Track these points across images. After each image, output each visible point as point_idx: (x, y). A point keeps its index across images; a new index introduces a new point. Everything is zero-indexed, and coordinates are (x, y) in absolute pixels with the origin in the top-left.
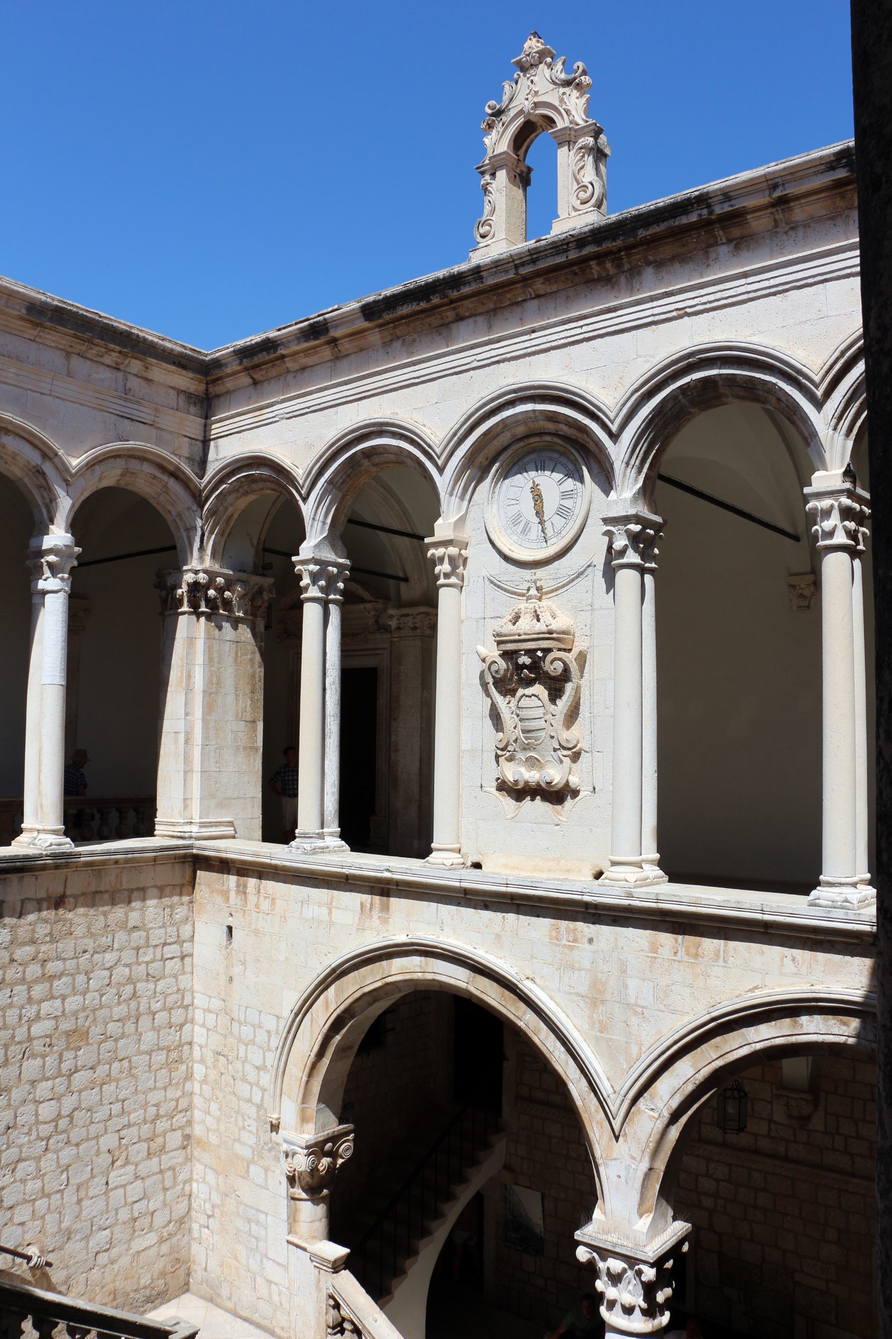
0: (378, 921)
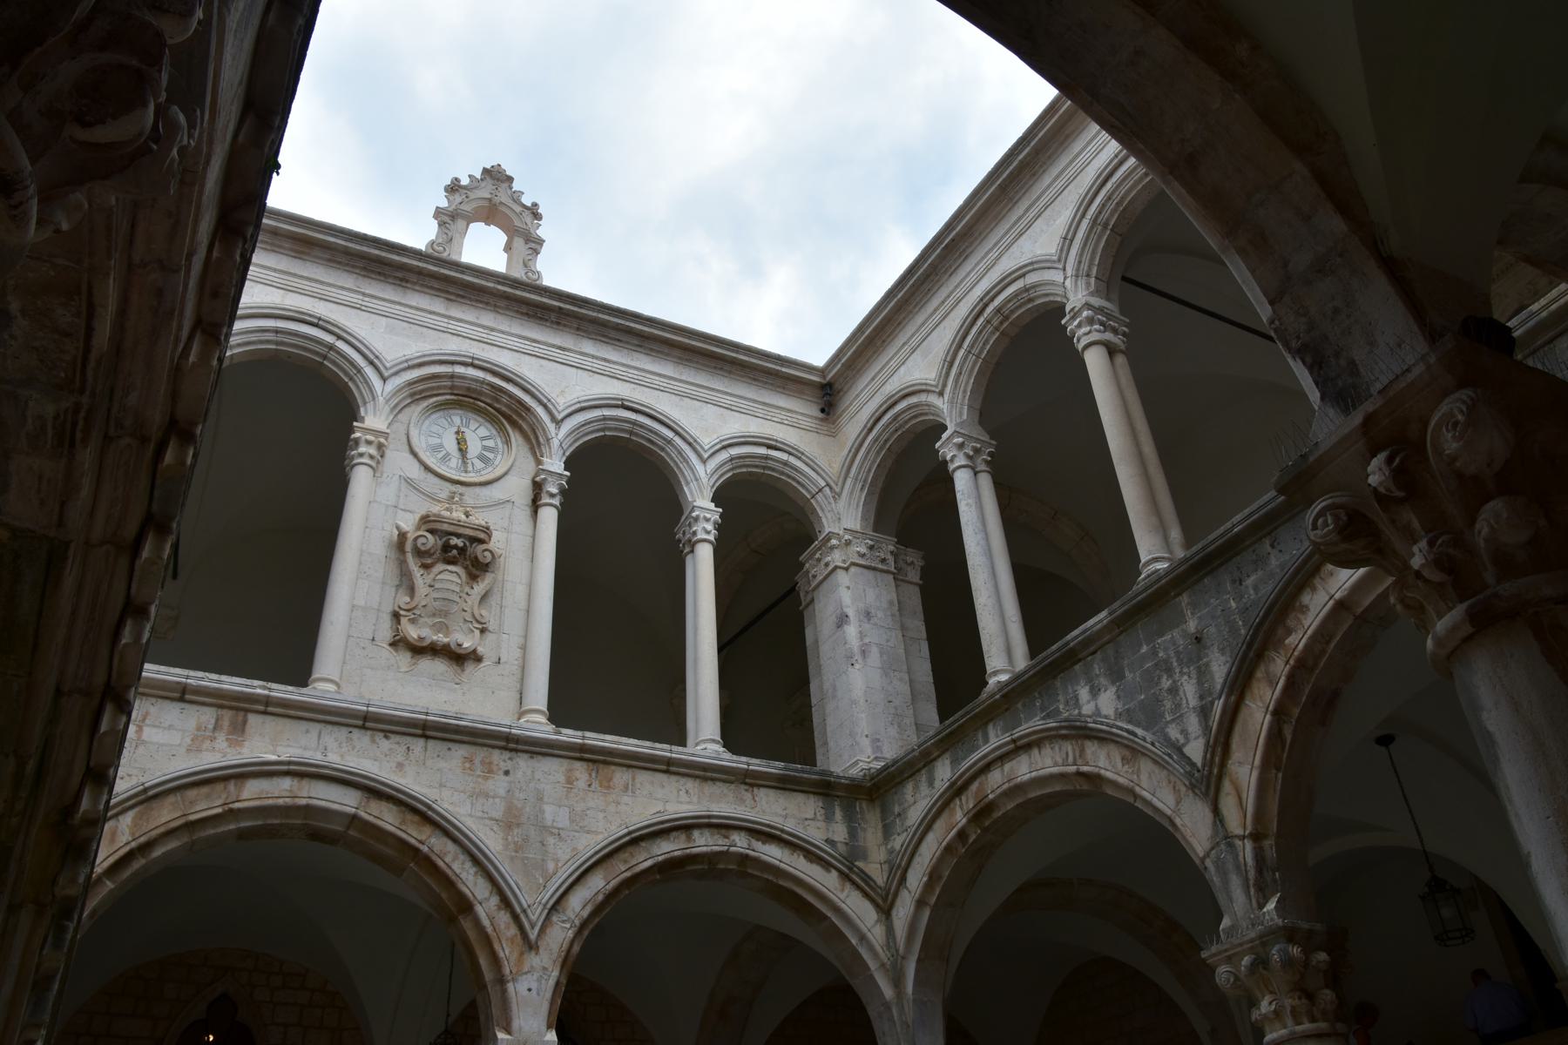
0: (225, 744)
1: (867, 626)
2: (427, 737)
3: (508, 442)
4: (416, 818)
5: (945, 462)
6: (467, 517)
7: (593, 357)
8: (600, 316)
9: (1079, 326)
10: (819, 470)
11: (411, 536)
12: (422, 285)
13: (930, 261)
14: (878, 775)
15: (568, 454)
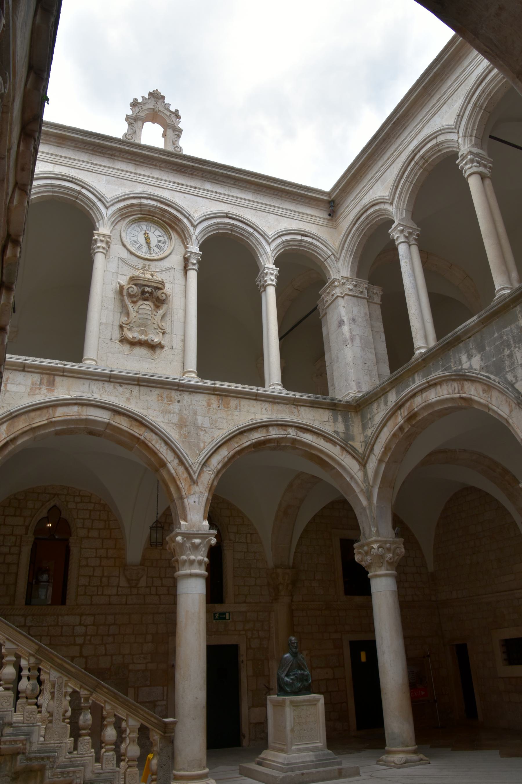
0: (46, 391)
1: (353, 326)
2: (140, 385)
3: (170, 238)
4: (137, 424)
5: (393, 241)
6: (152, 277)
7: (211, 191)
8: (213, 169)
9: (466, 164)
10: (329, 247)
11: (126, 288)
12: (122, 158)
13: (385, 131)
14: (359, 400)
15: (200, 243)
